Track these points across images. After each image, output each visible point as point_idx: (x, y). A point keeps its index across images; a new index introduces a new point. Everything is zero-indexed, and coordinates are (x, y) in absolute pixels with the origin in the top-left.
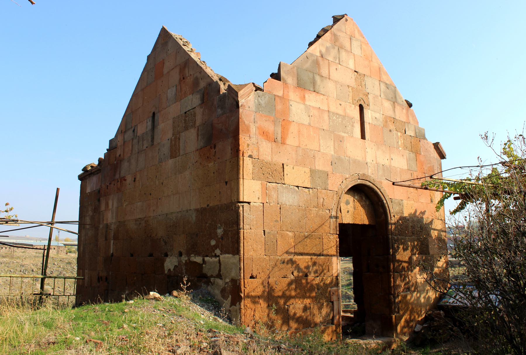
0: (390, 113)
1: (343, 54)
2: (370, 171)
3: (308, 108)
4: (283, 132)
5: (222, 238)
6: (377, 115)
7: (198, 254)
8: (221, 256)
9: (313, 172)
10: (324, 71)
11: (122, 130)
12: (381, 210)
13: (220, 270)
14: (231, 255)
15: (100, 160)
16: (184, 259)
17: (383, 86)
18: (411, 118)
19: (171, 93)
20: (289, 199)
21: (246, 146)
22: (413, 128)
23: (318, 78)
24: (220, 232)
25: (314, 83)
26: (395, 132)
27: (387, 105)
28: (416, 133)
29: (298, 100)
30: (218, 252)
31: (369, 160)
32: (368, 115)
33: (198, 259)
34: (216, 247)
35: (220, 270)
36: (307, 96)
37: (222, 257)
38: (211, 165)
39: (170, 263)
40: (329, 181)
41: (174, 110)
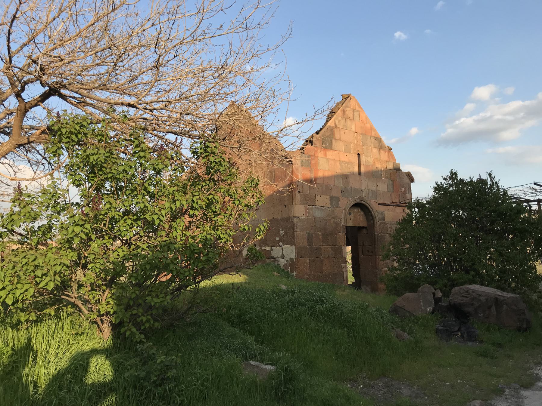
1: (348, 121)
3: (328, 160)
5: (283, 236)
7: (267, 245)
8: (283, 246)
9: (331, 198)
10: (337, 136)
12: (371, 218)
13: (283, 254)
14: (289, 246)
17: (373, 140)
20: (319, 214)
23: (334, 141)
27: (375, 151)
29: (323, 156)
30: (281, 244)
31: (363, 188)
33: (268, 248)
34: (279, 241)
35: (283, 254)
36: (327, 153)
37: (283, 246)
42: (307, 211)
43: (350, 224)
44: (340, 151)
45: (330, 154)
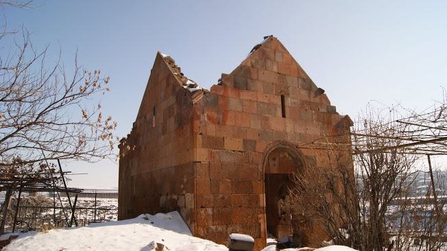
0: (306, 98)
1: (269, 63)
2: (289, 138)
3: (241, 102)
4: (223, 117)
6: (295, 101)
7: (175, 194)
9: (245, 141)
10: (254, 77)
11: (139, 118)
15: (128, 135)
16: (169, 197)
17: (300, 81)
18: (324, 101)
19: (162, 94)
20: (226, 159)
21: (198, 128)
22: (325, 107)
23: (249, 81)
24: (185, 180)
25: (247, 84)
26: (310, 111)
27: (304, 92)
28: (328, 109)
29: (234, 96)
31: (288, 130)
32: (288, 101)
33: (175, 197)
34: (183, 189)
36: (241, 93)
38: (181, 139)
39: (163, 199)
40: (257, 147)
41: (164, 105)
42: (211, 155)
43: (274, 171)
44: (257, 91)
45: (245, 95)
